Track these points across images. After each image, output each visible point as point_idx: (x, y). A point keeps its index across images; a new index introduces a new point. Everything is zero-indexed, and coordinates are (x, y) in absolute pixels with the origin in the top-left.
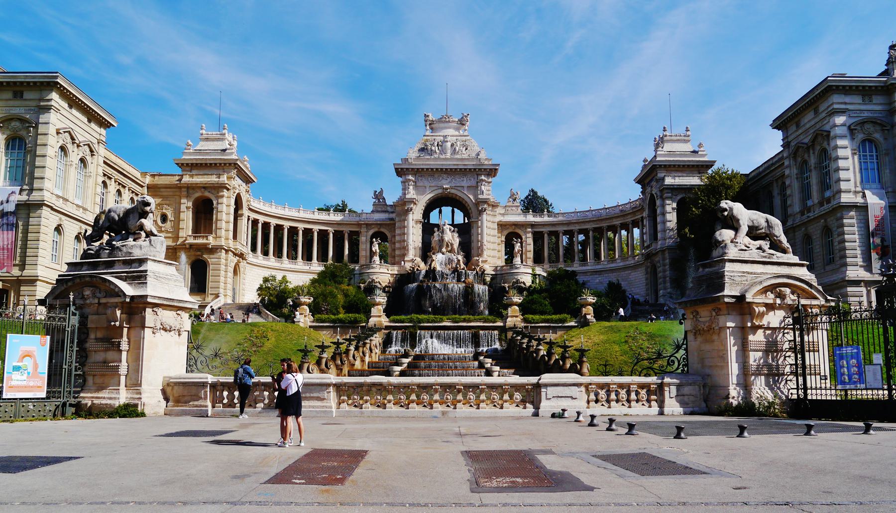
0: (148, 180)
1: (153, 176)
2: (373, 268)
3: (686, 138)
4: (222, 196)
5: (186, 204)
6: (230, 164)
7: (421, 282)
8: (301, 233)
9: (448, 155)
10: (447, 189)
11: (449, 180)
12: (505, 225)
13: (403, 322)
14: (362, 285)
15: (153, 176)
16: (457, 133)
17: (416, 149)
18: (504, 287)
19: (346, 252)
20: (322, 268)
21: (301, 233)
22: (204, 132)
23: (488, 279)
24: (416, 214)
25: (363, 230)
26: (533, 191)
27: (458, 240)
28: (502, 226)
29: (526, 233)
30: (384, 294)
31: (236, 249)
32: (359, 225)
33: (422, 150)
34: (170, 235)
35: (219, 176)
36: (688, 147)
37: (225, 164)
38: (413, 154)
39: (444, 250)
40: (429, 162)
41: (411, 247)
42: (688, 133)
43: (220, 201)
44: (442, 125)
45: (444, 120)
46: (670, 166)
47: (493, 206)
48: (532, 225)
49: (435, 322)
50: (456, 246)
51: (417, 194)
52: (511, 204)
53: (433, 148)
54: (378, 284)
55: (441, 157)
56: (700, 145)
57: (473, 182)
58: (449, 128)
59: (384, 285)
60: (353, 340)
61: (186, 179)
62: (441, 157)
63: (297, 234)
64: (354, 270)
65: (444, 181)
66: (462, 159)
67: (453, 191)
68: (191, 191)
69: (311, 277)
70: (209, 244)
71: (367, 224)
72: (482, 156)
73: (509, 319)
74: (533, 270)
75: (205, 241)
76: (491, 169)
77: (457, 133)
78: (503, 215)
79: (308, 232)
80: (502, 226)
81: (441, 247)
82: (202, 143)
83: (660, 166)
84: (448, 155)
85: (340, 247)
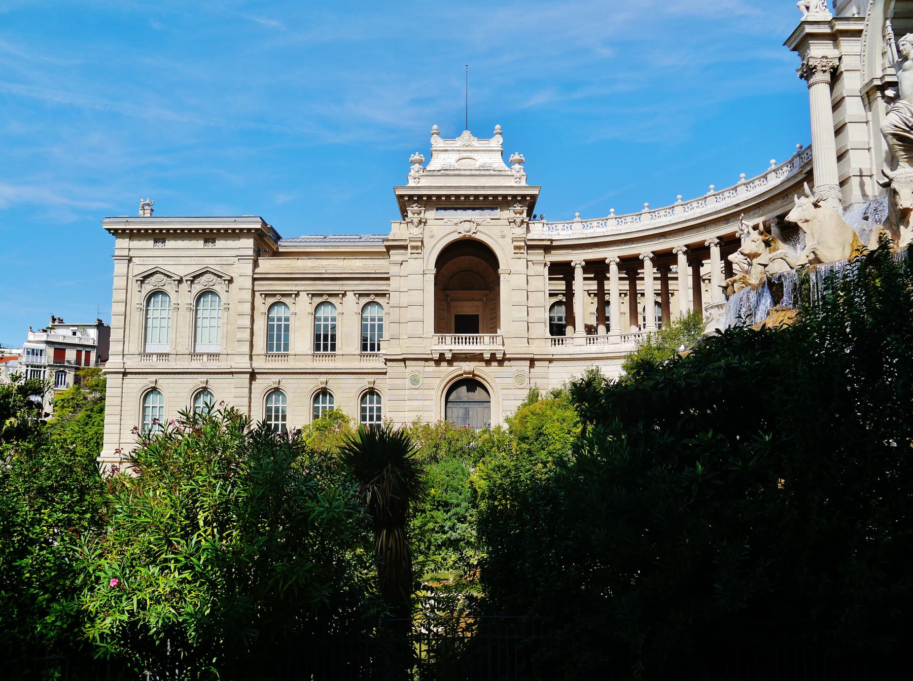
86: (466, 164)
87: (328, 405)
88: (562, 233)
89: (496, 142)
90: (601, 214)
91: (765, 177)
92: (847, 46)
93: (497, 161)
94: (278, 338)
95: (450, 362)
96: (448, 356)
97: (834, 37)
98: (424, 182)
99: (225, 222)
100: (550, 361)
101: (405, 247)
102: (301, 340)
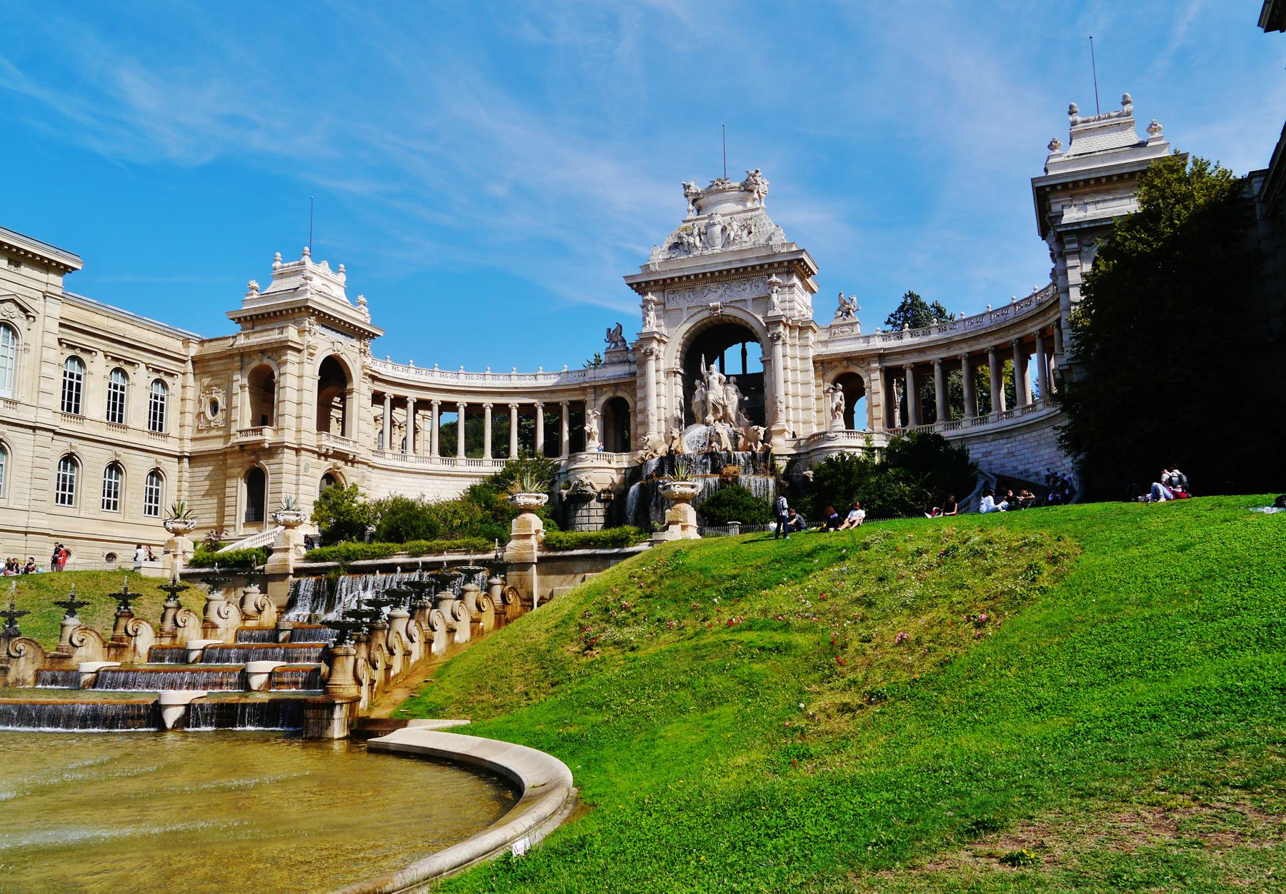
0: (194, 350)
1: (202, 342)
2: (582, 460)
3: (1123, 120)
4: (285, 363)
5: (241, 380)
6: (300, 308)
7: (648, 477)
8: (488, 413)
9: (718, 248)
10: (716, 308)
11: (720, 292)
12: (830, 362)
13: (323, 560)
14: (565, 492)
15: (202, 342)
16: (740, 208)
17: (666, 246)
18: (806, 477)
19: (566, 437)
20: (498, 469)
21: (488, 413)
22: (278, 264)
23: (782, 464)
24: (668, 356)
25: (589, 398)
26: (911, 295)
27: (735, 399)
28: (822, 364)
29: (869, 371)
30: (600, 505)
31: (320, 447)
32: (583, 389)
33: (675, 246)
34: (221, 433)
35: (282, 329)
36: (1131, 137)
37: (293, 309)
38: (658, 256)
39: (710, 418)
40: (687, 265)
41: (653, 419)
42: (1128, 108)
43: (282, 370)
44: (712, 198)
45: (715, 189)
46: (1076, 183)
47: (801, 328)
48: (881, 356)
49: (379, 557)
50: (732, 410)
51: (668, 325)
52: (840, 321)
53: (691, 240)
54: (589, 489)
55: (705, 252)
56: (1152, 128)
57: (760, 291)
58: (726, 201)
59: (599, 489)
60: (405, 594)
61: (242, 341)
62: (705, 252)
63: (483, 415)
64: (559, 466)
65: (711, 296)
66: (741, 251)
67: (728, 311)
68: (246, 360)
69: (467, 483)
70: (263, 441)
71: (595, 387)
72: (776, 241)
73: (512, 543)
74: (868, 440)
75: (259, 437)
76: (790, 262)
77: (740, 208)
78: (825, 343)
79: (501, 411)
80: (822, 364)
81: (705, 413)
82: (275, 282)
83: (1053, 187)
84: (718, 248)
85: (547, 429)
86: (325, 289)
87: (113, 480)
88: (387, 370)
89: (342, 278)
90: (406, 363)
91: (536, 376)
92: (662, 347)
93: (339, 293)
94: (72, 399)
95: (326, 456)
96: (331, 452)
97: (660, 341)
98: (316, 298)
99: (31, 245)
100: (374, 467)
101: (299, 351)
102: (95, 403)
